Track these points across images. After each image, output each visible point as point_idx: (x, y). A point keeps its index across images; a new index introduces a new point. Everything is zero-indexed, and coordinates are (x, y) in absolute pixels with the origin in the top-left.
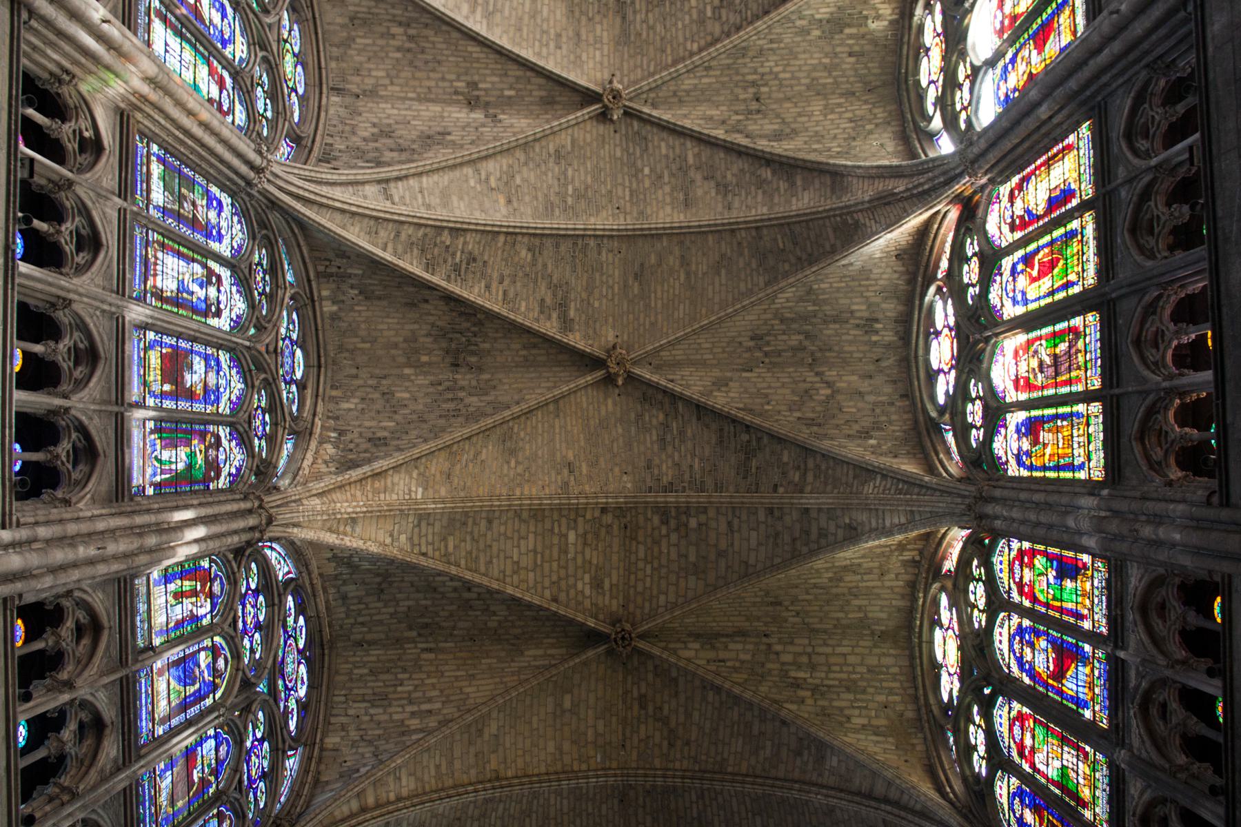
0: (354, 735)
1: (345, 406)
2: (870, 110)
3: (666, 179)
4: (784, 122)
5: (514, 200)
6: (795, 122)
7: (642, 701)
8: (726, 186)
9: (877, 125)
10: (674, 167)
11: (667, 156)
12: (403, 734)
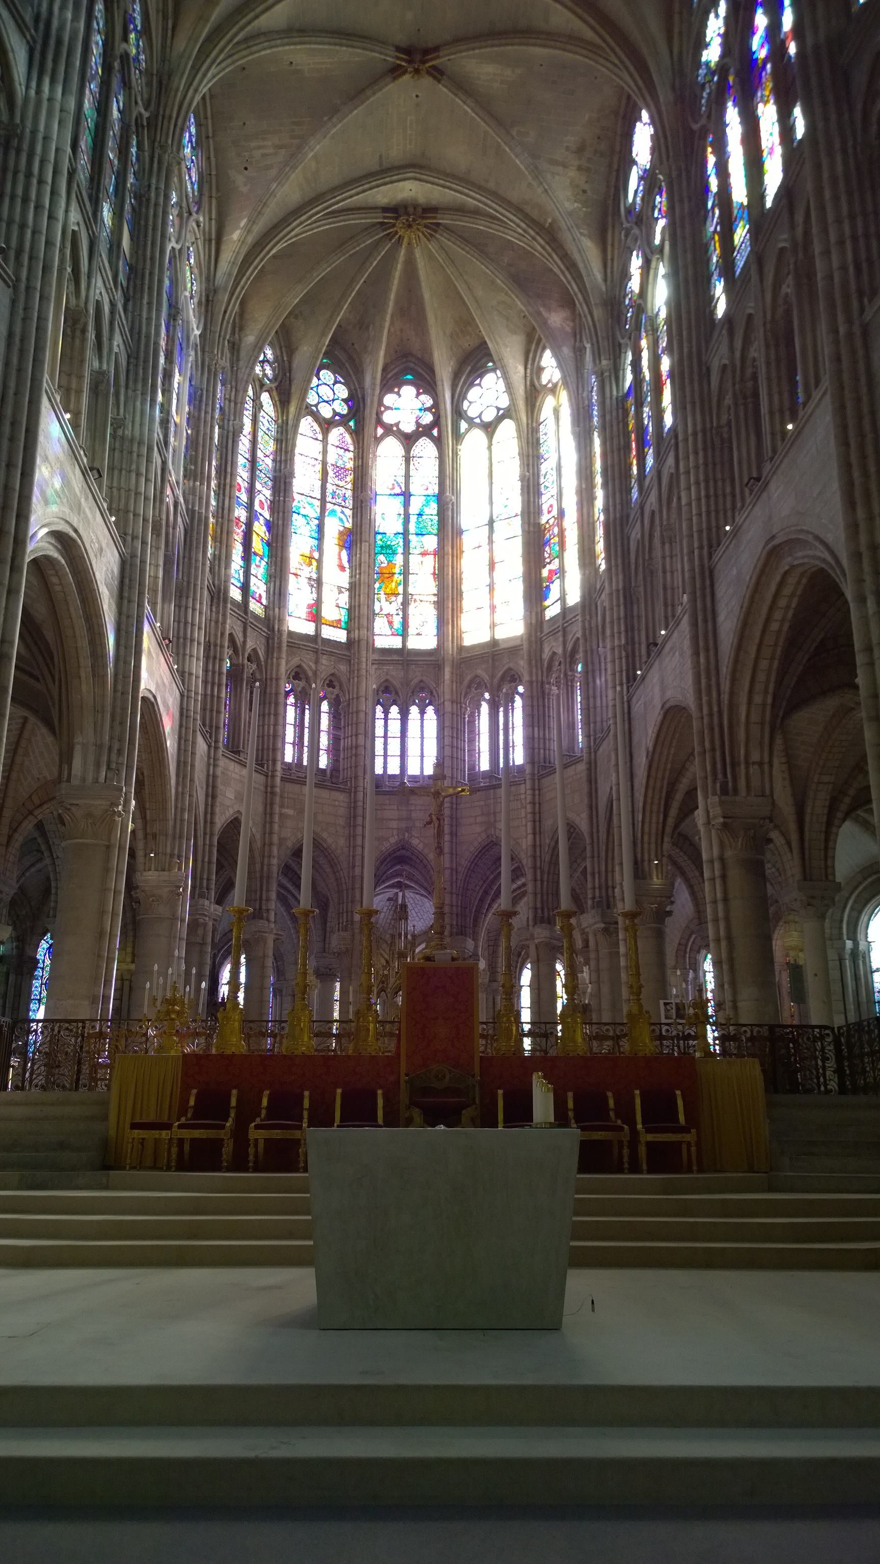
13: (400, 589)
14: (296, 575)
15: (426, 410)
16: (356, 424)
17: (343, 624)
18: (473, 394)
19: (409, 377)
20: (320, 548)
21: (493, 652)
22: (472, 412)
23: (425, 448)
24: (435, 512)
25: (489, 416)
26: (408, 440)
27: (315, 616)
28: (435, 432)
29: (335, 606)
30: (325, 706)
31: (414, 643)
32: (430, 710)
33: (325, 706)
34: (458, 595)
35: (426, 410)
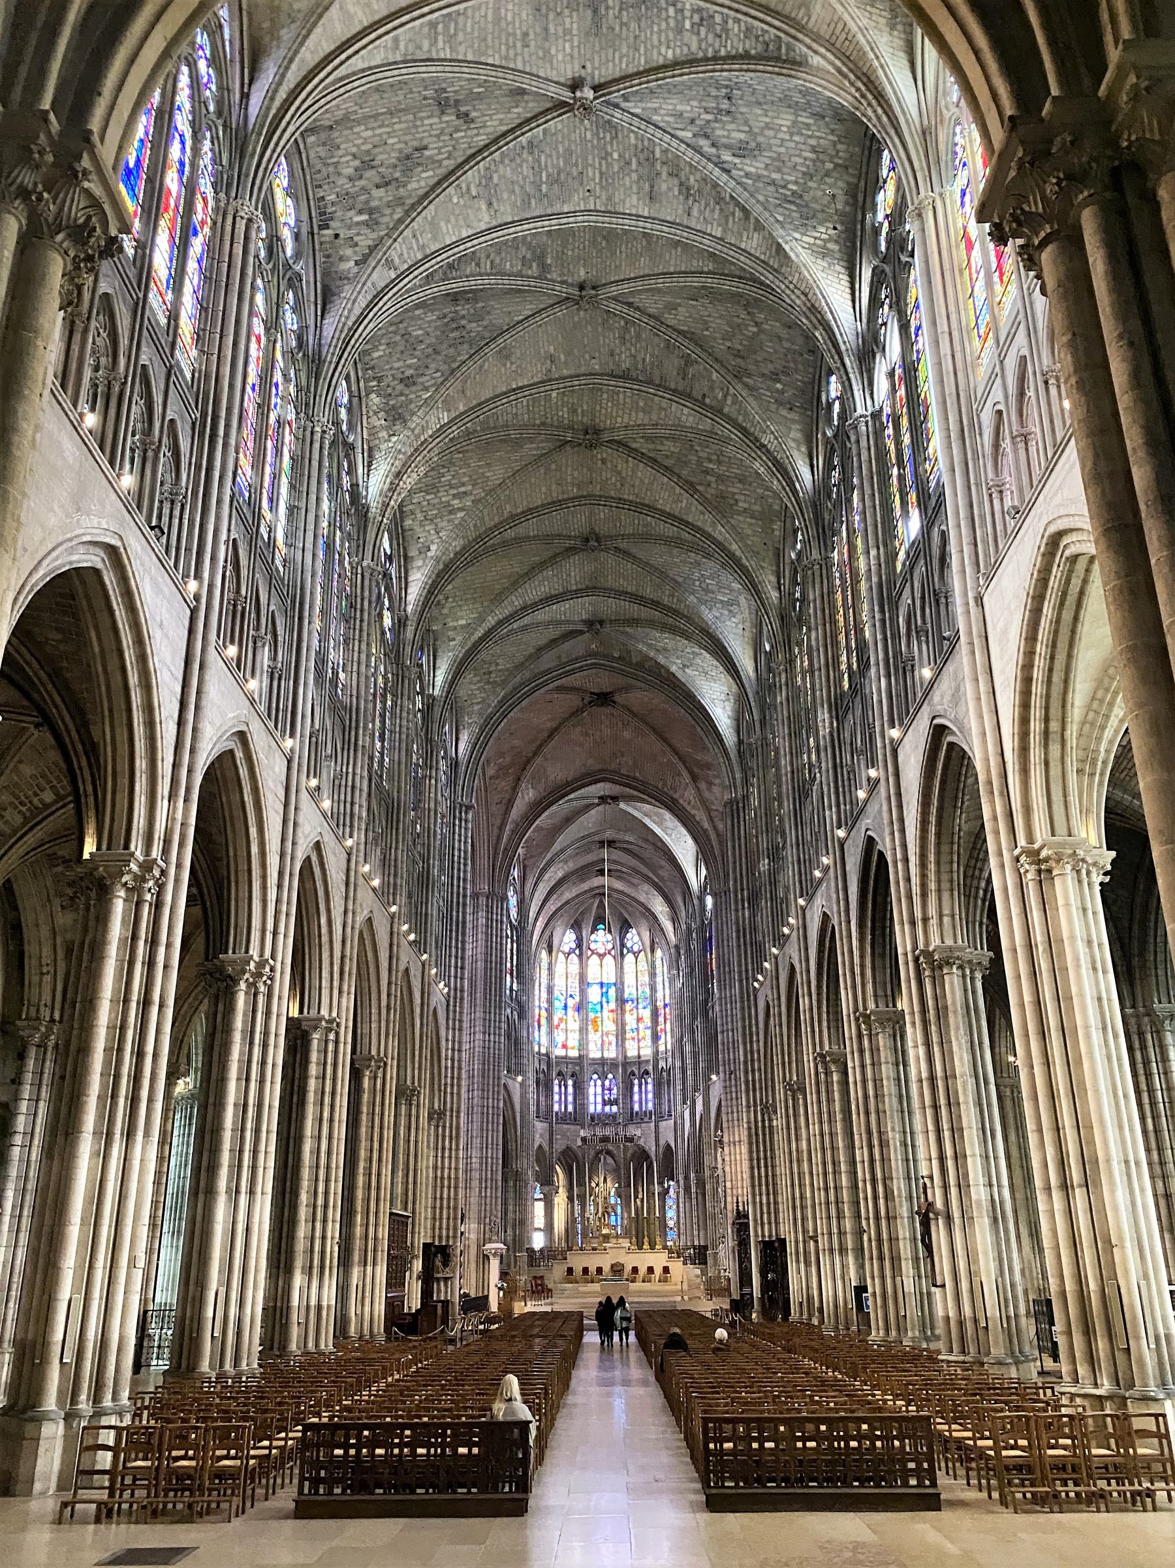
0: (420, 516)
1: (376, 355)
2: (834, 143)
3: (634, 166)
4: (750, 131)
5: (494, 200)
6: (762, 134)
7: (603, 461)
8: (688, 189)
9: (836, 165)
10: (642, 157)
11: (636, 146)
12: (451, 512)
18: (629, 936)
21: (639, 1061)
22: (629, 944)
23: (609, 960)
25: (636, 948)
26: (601, 956)
27: (564, 1046)
29: (573, 1040)
30: (570, 1082)
33: (570, 1082)
34: (624, 1032)
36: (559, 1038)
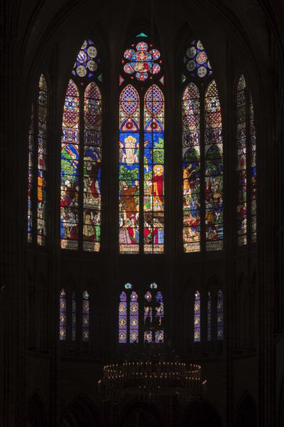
13: (138, 207)
14: (65, 207)
15: (157, 62)
16: (103, 78)
17: (98, 239)
19: (143, 35)
20: (82, 187)
23: (156, 95)
24: (162, 146)
26: (142, 87)
28: (162, 80)
29: (93, 226)
31: (148, 249)
32: (159, 296)
35: (157, 62)
36: (67, 221)
